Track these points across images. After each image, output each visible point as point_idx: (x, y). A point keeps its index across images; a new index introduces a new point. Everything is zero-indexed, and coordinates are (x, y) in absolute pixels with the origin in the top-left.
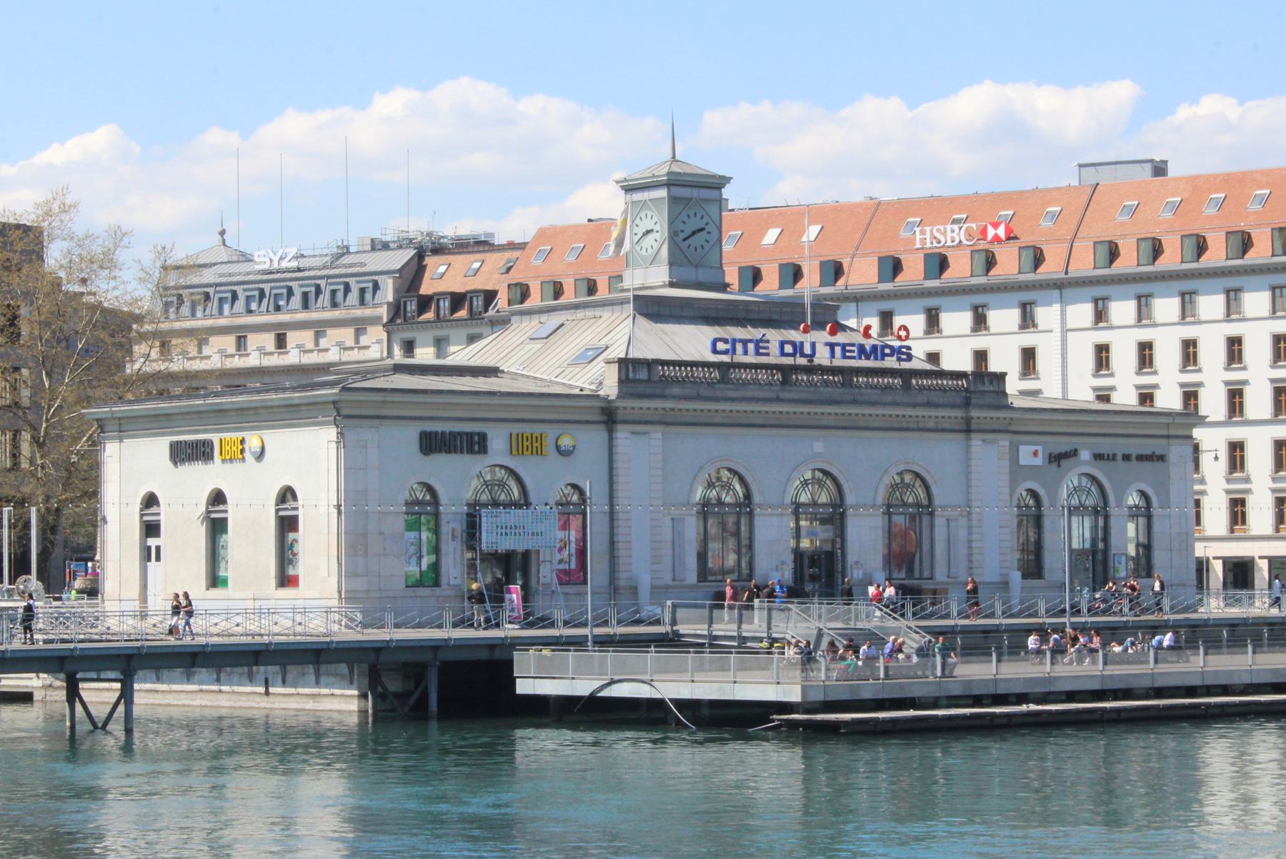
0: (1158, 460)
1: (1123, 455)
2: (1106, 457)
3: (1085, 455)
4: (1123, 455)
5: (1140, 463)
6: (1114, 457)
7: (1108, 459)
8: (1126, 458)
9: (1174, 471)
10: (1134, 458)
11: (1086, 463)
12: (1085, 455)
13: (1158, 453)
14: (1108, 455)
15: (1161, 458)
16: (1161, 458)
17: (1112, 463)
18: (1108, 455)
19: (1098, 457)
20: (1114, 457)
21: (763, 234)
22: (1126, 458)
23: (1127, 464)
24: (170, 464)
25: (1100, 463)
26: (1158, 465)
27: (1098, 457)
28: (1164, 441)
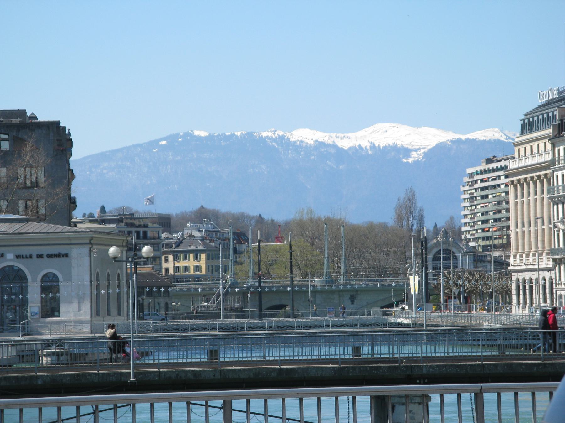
0: (63, 256)
1: (37, 255)
2: (25, 256)
3: (10, 256)
4: (37, 255)
5: (50, 259)
6: (31, 256)
7: (27, 257)
8: (40, 256)
9: (74, 262)
10: (45, 256)
11: (10, 260)
12: (10, 256)
13: (63, 252)
14: (26, 255)
15: (66, 255)
16: (66, 255)
17: (30, 260)
18: (26, 255)
19: (18, 257)
20: (31, 256)
21: (164, 145)
22: (40, 256)
23: (40, 259)
24: (104, 206)
25: (22, 260)
26: (65, 258)
27: (18, 257)
28: (67, 247)
